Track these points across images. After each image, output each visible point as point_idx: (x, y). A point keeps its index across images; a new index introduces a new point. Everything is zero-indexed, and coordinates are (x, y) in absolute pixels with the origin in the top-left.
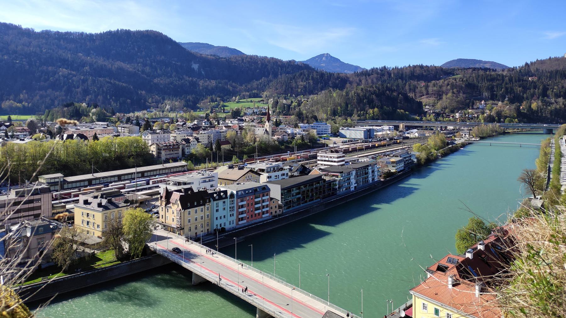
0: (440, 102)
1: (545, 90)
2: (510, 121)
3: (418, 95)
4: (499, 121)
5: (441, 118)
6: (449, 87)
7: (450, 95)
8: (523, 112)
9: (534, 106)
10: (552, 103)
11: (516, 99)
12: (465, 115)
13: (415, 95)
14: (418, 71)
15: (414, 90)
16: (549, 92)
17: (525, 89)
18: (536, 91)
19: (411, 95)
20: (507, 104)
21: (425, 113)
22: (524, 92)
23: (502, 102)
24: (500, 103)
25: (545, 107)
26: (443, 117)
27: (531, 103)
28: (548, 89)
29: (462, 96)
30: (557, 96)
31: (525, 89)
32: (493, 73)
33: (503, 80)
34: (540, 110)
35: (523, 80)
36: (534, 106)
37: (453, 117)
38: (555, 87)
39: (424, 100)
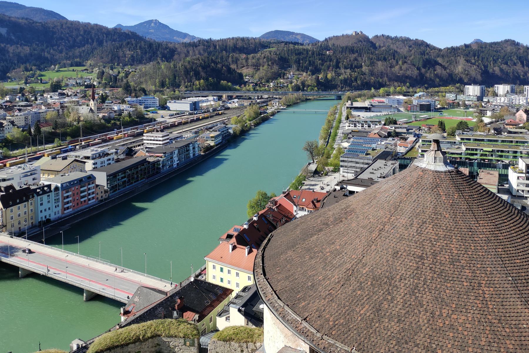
0: (258, 73)
1: (338, 63)
2: (312, 89)
3: (240, 66)
4: (303, 90)
5: (258, 88)
6: (265, 60)
7: (266, 67)
8: (321, 82)
9: (329, 76)
10: (342, 74)
11: (316, 71)
12: (278, 84)
13: (237, 66)
14: (240, 44)
15: (236, 61)
16: (340, 65)
17: (324, 61)
18: (331, 63)
19: (233, 66)
20: (310, 75)
21: (245, 83)
22: (322, 65)
23: (307, 73)
24: (305, 74)
25: (337, 77)
26: (260, 86)
27: (327, 74)
28: (340, 62)
29: (276, 68)
30: (346, 68)
31: (324, 61)
32: (301, 47)
33: (307, 53)
34: (333, 79)
35: (322, 54)
36: (329, 76)
37: (268, 86)
38: (345, 60)
39: (245, 71)
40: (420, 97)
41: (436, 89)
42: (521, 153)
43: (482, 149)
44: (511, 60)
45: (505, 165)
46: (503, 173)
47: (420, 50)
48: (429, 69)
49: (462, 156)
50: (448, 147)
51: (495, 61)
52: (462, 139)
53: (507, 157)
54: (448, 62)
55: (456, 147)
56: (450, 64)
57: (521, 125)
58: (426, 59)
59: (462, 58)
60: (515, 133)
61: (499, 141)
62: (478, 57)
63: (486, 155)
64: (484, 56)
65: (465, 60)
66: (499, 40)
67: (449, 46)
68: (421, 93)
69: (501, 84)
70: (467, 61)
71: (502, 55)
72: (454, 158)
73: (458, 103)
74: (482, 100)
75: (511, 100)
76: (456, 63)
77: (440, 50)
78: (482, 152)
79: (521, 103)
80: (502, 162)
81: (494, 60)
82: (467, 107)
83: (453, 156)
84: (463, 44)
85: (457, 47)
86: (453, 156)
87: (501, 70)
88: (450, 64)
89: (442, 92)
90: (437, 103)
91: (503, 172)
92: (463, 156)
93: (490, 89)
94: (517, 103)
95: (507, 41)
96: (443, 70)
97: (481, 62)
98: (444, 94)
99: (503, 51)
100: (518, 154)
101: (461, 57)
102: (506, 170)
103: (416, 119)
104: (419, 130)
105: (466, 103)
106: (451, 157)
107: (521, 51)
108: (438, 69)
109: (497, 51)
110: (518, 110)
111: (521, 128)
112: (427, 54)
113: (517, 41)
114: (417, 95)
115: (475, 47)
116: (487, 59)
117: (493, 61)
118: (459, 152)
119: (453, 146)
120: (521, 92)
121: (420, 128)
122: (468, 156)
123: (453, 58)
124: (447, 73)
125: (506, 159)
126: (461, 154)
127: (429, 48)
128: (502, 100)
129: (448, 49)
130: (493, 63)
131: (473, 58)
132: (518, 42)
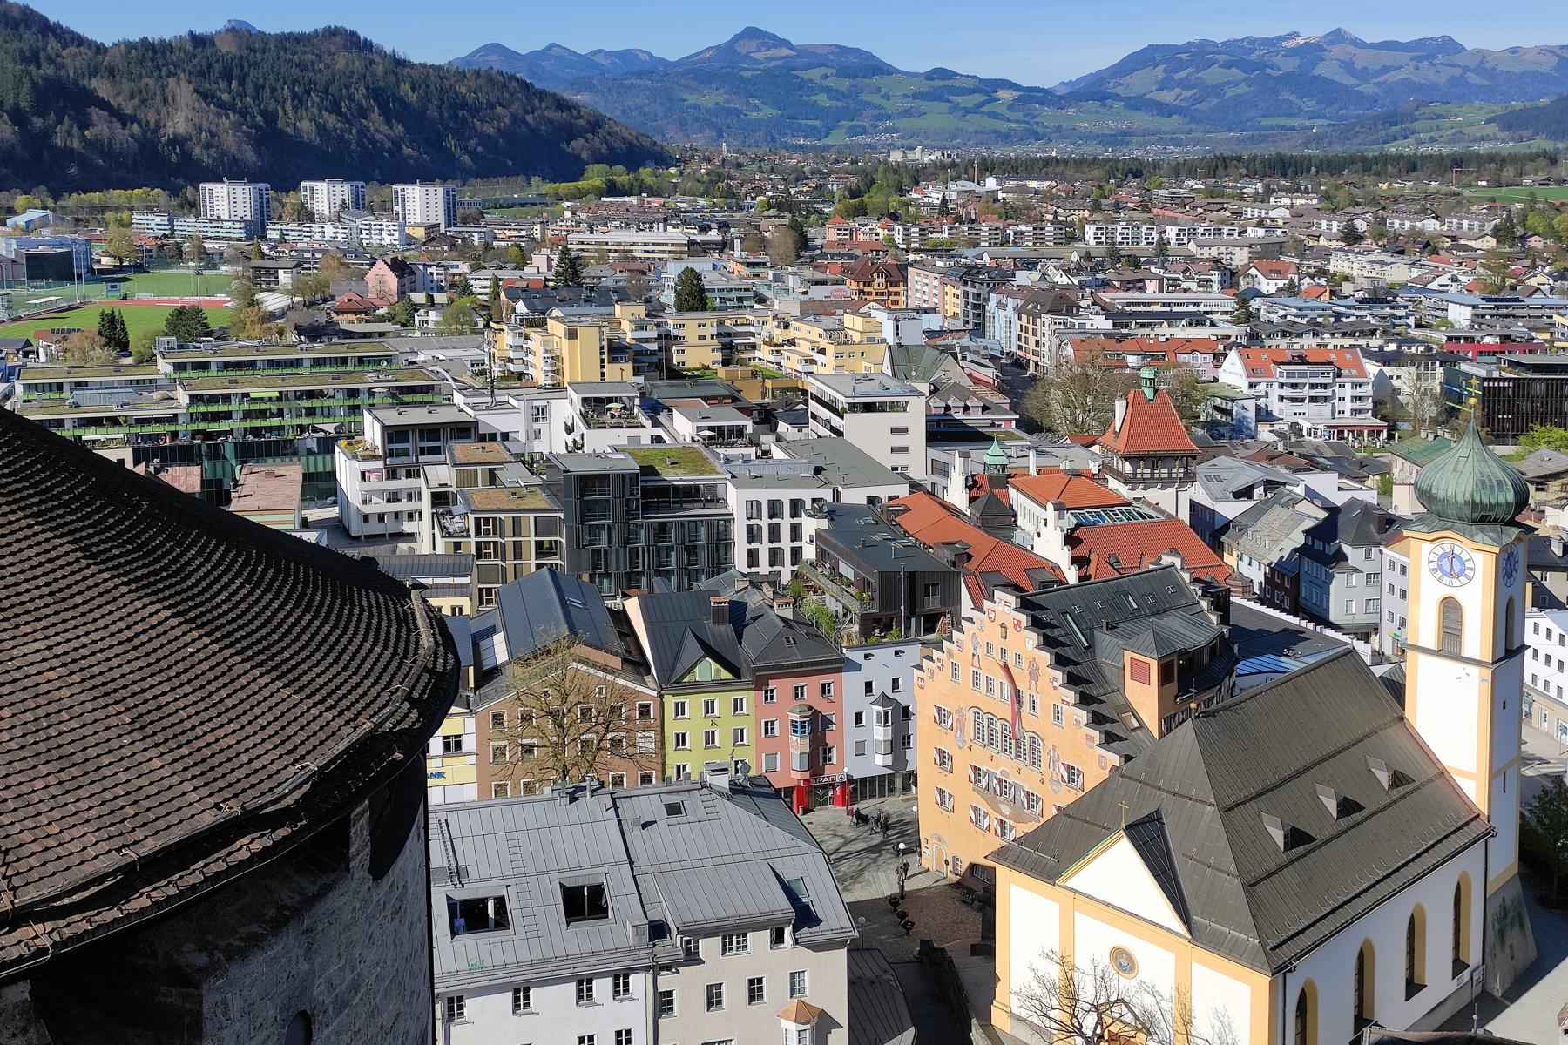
40: (29, 227)
41: (95, 197)
42: (371, 393)
43: (247, 395)
44: (351, 98)
45: (326, 438)
46: (320, 469)
47: (16, 44)
48: (60, 122)
49: (179, 428)
50: (124, 398)
51: (299, 101)
52: (179, 367)
53: (329, 413)
54: (132, 97)
55: (157, 395)
56: (144, 101)
57: (380, 312)
58: (46, 79)
59: (184, 83)
60: (365, 335)
61: (306, 364)
62: (242, 83)
63: (262, 414)
64: (261, 81)
65: (196, 91)
66: (308, 29)
67: (135, 37)
68: (32, 215)
69: (322, 180)
70: (206, 96)
71: (321, 79)
72: (149, 437)
73: (179, 247)
74: (263, 236)
75: (354, 231)
76: (165, 101)
77: (100, 49)
78: (245, 407)
79: (387, 240)
80: (316, 430)
81: (294, 95)
82: (209, 260)
83: (147, 430)
84: (184, 32)
85: (162, 41)
86: (147, 430)
87: (322, 129)
88: (144, 101)
89: (118, 209)
90: (97, 249)
91: (319, 464)
92: (182, 427)
93: (291, 199)
94: (375, 243)
95: (332, 32)
96: (119, 125)
97: (255, 99)
98: (125, 215)
99: (321, 66)
100: (363, 400)
101: (179, 80)
102: (328, 458)
103: (14, 314)
104: (26, 355)
105: (206, 246)
106: (137, 435)
107: (380, 69)
108: (94, 118)
109: (302, 67)
110: (373, 264)
111: (382, 319)
112: (50, 60)
113: (363, 33)
114: (21, 220)
115: (227, 47)
116: (274, 90)
117: (293, 100)
118: (169, 412)
119: (145, 394)
120: (385, 208)
121: (28, 343)
122: (202, 426)
123: (151, 82)
124: (132, 136)
125: (326, 420)
126: (174, 419)
127: (55, 35)
128: (327, 233)
129: (130, 46)
130: (294, 107)
131: (223, 85)
132: (366, 40)
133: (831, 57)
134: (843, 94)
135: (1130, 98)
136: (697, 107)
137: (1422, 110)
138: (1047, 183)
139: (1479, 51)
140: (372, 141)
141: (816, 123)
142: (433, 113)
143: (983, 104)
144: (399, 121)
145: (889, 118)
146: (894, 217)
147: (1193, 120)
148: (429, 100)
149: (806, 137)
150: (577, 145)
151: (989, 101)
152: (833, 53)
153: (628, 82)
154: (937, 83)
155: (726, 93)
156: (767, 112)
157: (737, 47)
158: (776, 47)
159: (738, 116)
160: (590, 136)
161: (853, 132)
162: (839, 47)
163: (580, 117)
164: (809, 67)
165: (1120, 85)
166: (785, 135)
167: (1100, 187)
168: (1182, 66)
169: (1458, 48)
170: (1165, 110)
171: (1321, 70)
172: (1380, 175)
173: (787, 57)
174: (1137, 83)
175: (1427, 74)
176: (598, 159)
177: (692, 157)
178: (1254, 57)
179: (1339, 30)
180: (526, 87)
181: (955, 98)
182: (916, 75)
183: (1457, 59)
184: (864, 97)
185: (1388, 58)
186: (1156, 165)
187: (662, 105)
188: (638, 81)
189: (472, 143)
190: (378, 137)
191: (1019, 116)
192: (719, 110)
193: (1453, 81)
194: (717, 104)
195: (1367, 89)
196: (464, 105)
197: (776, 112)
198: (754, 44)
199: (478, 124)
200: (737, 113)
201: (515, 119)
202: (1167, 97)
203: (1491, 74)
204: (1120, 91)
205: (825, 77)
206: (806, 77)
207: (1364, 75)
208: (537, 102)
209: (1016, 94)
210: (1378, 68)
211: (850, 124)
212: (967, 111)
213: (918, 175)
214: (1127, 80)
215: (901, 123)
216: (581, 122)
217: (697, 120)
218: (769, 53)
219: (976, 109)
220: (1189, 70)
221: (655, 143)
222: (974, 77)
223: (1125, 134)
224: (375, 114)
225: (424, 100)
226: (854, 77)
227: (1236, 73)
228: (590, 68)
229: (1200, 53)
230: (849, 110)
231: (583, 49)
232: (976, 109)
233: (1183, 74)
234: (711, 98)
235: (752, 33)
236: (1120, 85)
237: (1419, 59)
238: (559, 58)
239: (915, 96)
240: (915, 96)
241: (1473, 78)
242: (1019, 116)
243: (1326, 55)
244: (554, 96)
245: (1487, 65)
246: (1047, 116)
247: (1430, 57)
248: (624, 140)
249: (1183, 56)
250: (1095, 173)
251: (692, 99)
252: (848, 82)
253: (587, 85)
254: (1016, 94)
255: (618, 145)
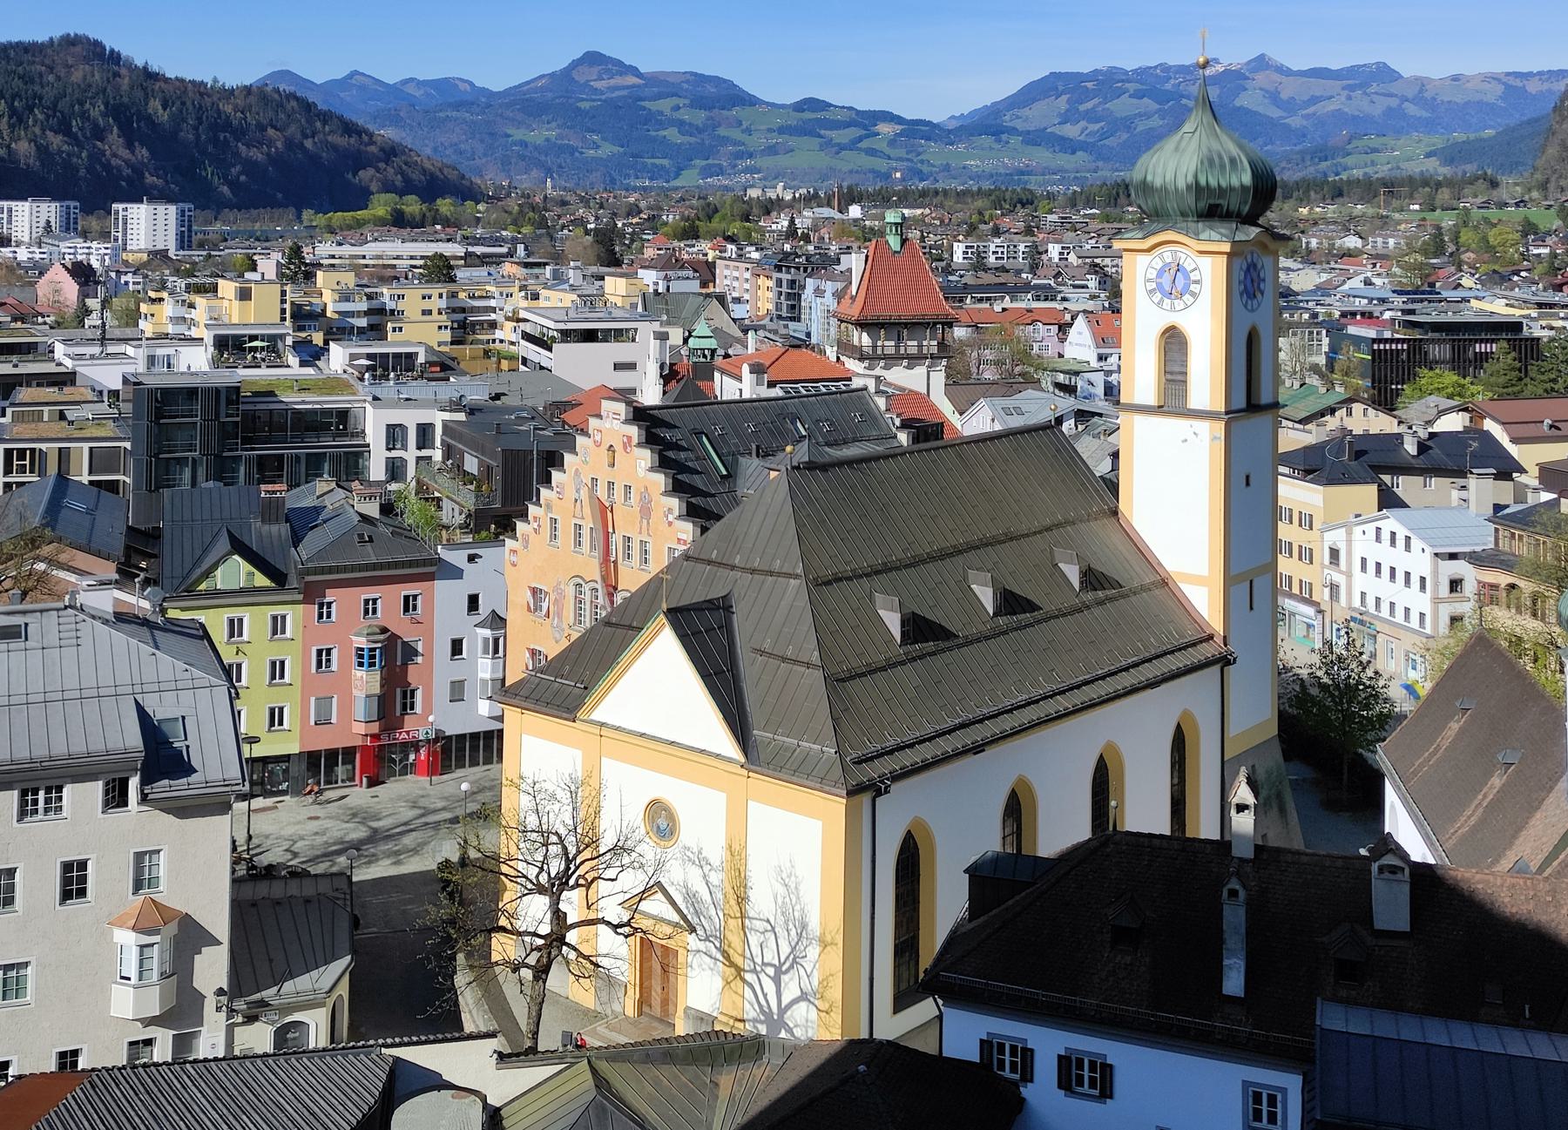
44: (84, 115)
66: (41, 37)
71: (49, 94)
75: (55, 256)
87: (43, 151)
95: (70, 42)
99: (51, 78)
109: (27, 79)
113: (109, 43)
117: (10, 117)
132: (112, 51)
133: (685, 86)
134: (697, 128)
135: (1028, 132)
136: (524, 144)
137: (1355, 143)
138: (919, 212)
139: (1417, 79)
140: (107, 167)
141: (665, 162)
142: (187, 135)
143: (860, 139)
144: (142, 145)
145: (751, 156)
146: (731, 239)
147: (1100, 157)
148: (184, 120)
149: (651, 179)
150: (366, 175)
151: (867, 136)
152: (687, 82)
153: (441, 115)
154: (808, 115)
155: (559, 127)
156: (607, 150)
157: (575, 74)
158: (621, 74)
159: (572, 154)
160: (382, 165)
161: (707, 172)
162: (695, 74)
163: (374, 143)
164: (659, 96)
165: (1018, 117)
166: (628, 176)
167: (980, 213)
168: (1087, 95)
169: (1394, 76)
170: (1069, 146)
171: (1243, 101)
172: (1302, 202)
173: (633, 86)
174: (1039, 115)
175: (1360, 105)
176: (388, 188)
177: (508, 195)
178: (1168, 86)
179: (1262, 56)
180: (307, 107)
181: (828, 133)
182: (783, 106)
183: (1394, 88)
184: (722, 132)
185: (1318, 87)
186: (1051, 197)
187: (482, 141)
188: (454, 114)
189: (234, 171)
190: (114, 162)
191: (902, 153)
192: (550, 147)
193: (1389, 112)
194: (547, 140)
195: (1295, 122)
196: (227, 125)
197: (617, 149)
198: (596, 70)
199: (242, 148)
200: (572, 150)
201: (290, 144)
202: (1071, 131)
203: (1431, 104)
204: (1019, 125)
205: (677, 108)
206: (654, 108)
207: (1290, 106)
208: (318, 124)
209: (898, 128)
210: (1306, 98)
211: (704, 163)
212: (842, 148)
213: (770, 207)
214: (1026, 112)
215: (765, 162)
216: (373, 149)
217: (523, 158)
218: (612, 82)
219: (852, 145)
220: (1096, 101)
221: (463, 177)
222: (851, 108)
223: (1022, 173)
224: (115, 139)
225: (178, 119)
226: (710, 109)
227: (1148, 104)
228: (398, 98)
229: (1108, 82)
230: (705, 147)
231: (391, 78)
232: (852, 145)
233: (1089, 105)
234: (541, 134)
235: (593, 59)
236: (1018, 117)
237: (1351, 88)
238: (362, 88)
239: (782, 130)
240: (782, 130)
241: (1411, 109)
242: (902, 153)
243: (1248, 84)
244: (341, 118)
245: (1427, 95)
246: (934, 153)
247: (1363, 86)
248: (424, 171)
249: (1090, 85)
250: (979, 203)
251: (518, 134)
252: (703, 114)
253: (394, 119)
254: (898, 128)
255: (415, 176)
